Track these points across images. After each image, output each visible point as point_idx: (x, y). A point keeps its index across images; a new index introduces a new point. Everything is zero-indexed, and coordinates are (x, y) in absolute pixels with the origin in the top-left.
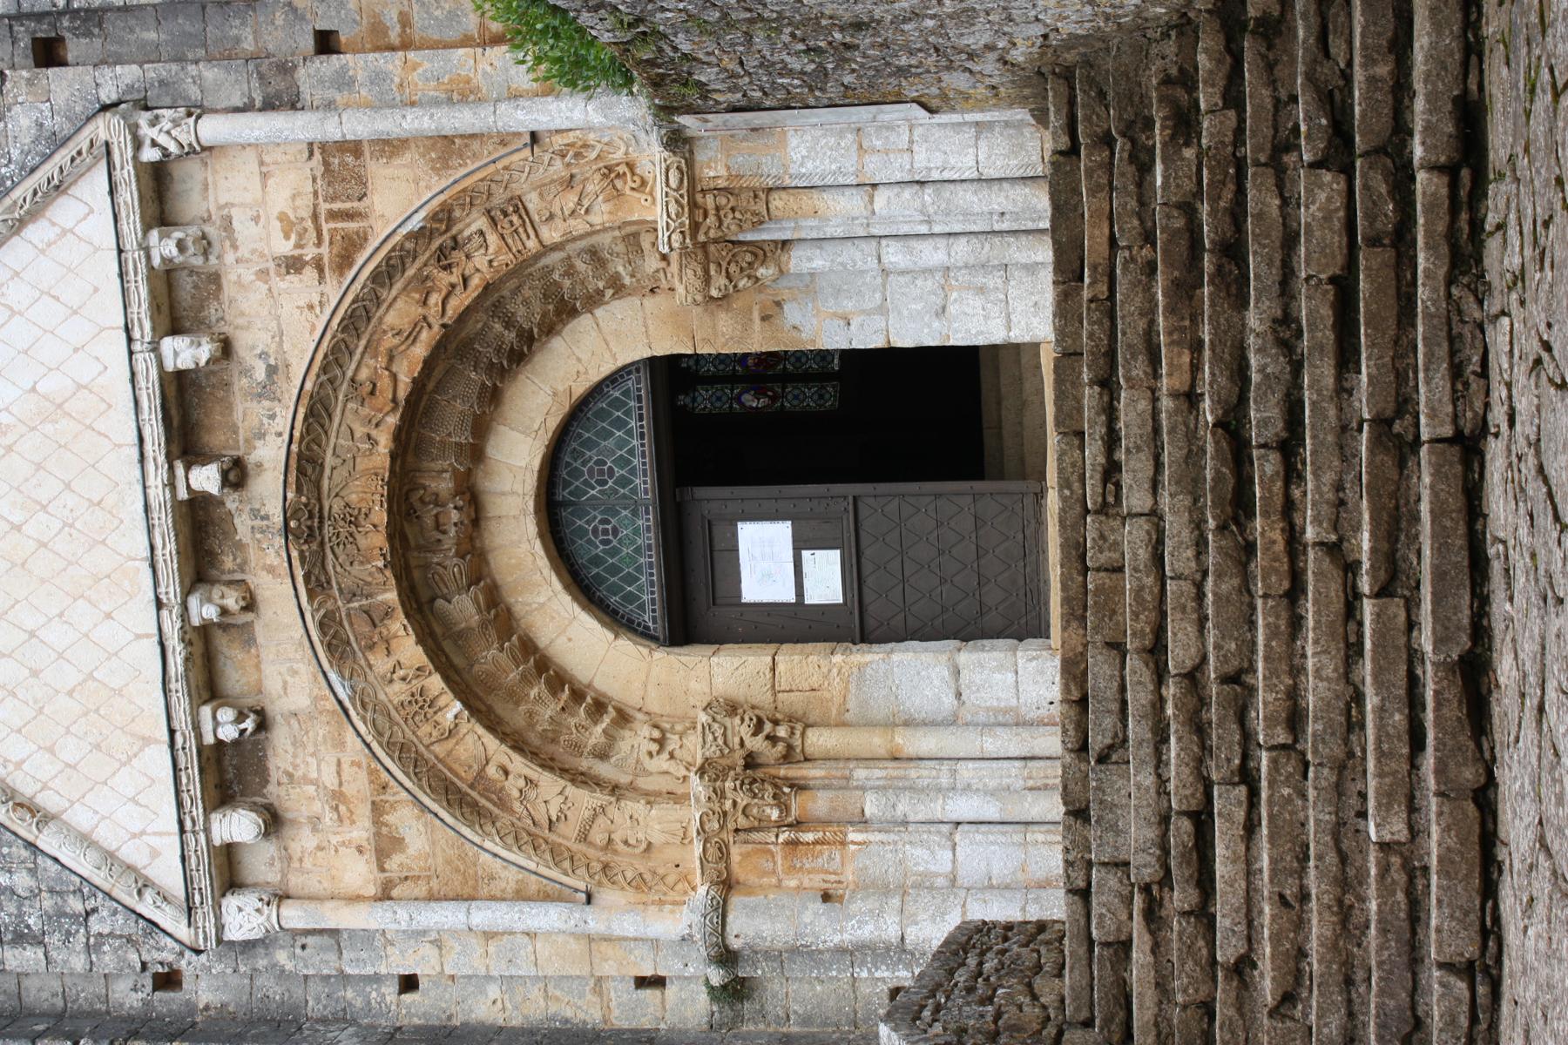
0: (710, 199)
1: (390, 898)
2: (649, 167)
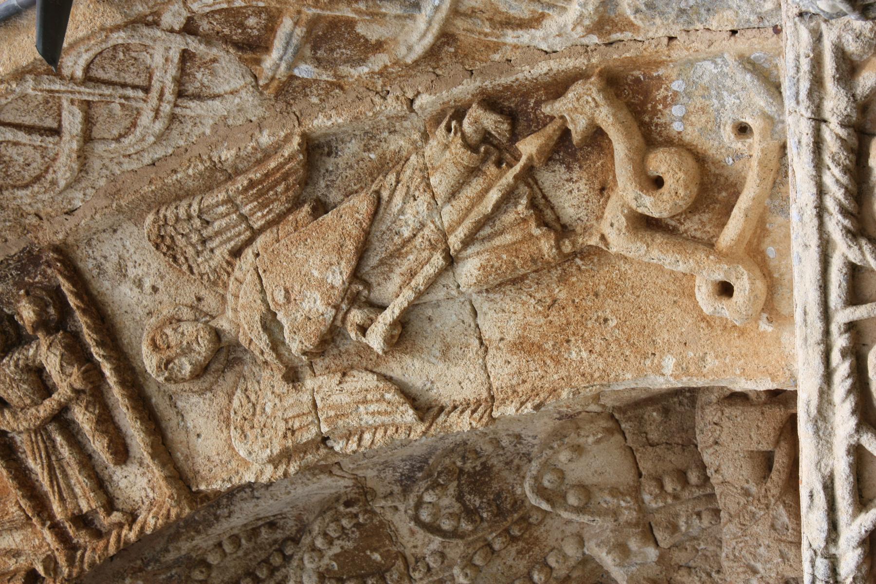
2: (747, 100)
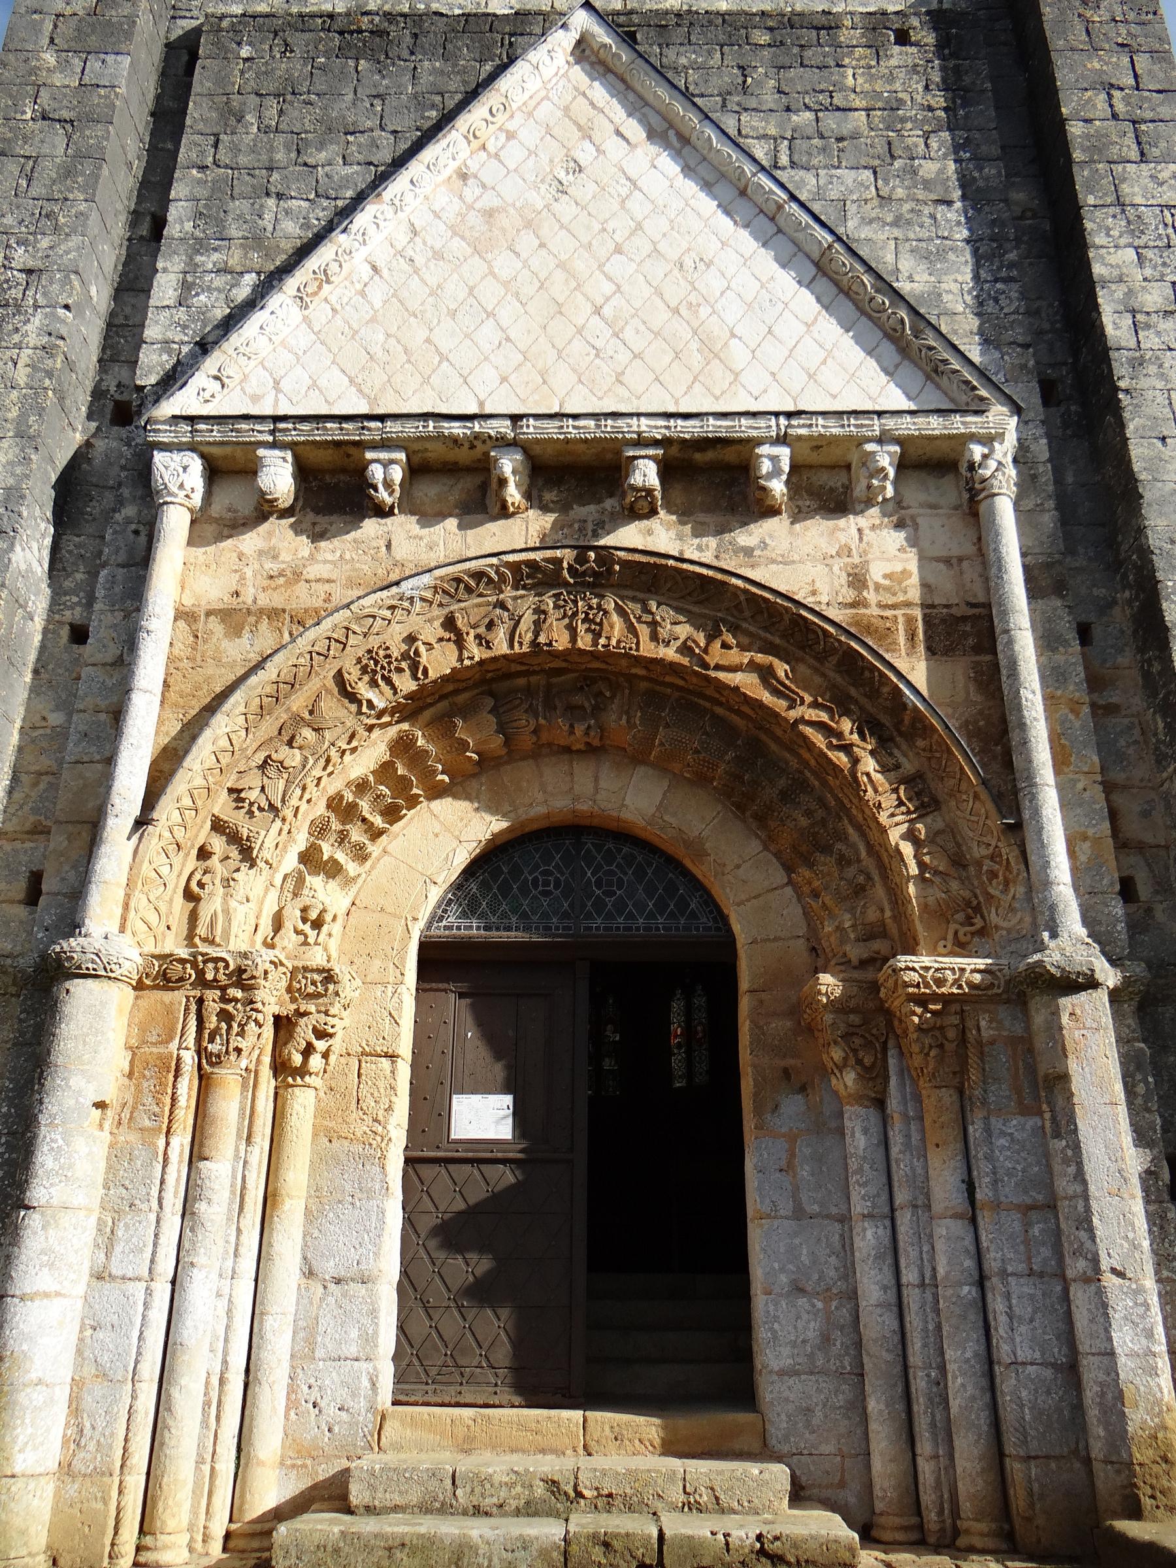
0: (955, 1020)
1: (176, 619)
